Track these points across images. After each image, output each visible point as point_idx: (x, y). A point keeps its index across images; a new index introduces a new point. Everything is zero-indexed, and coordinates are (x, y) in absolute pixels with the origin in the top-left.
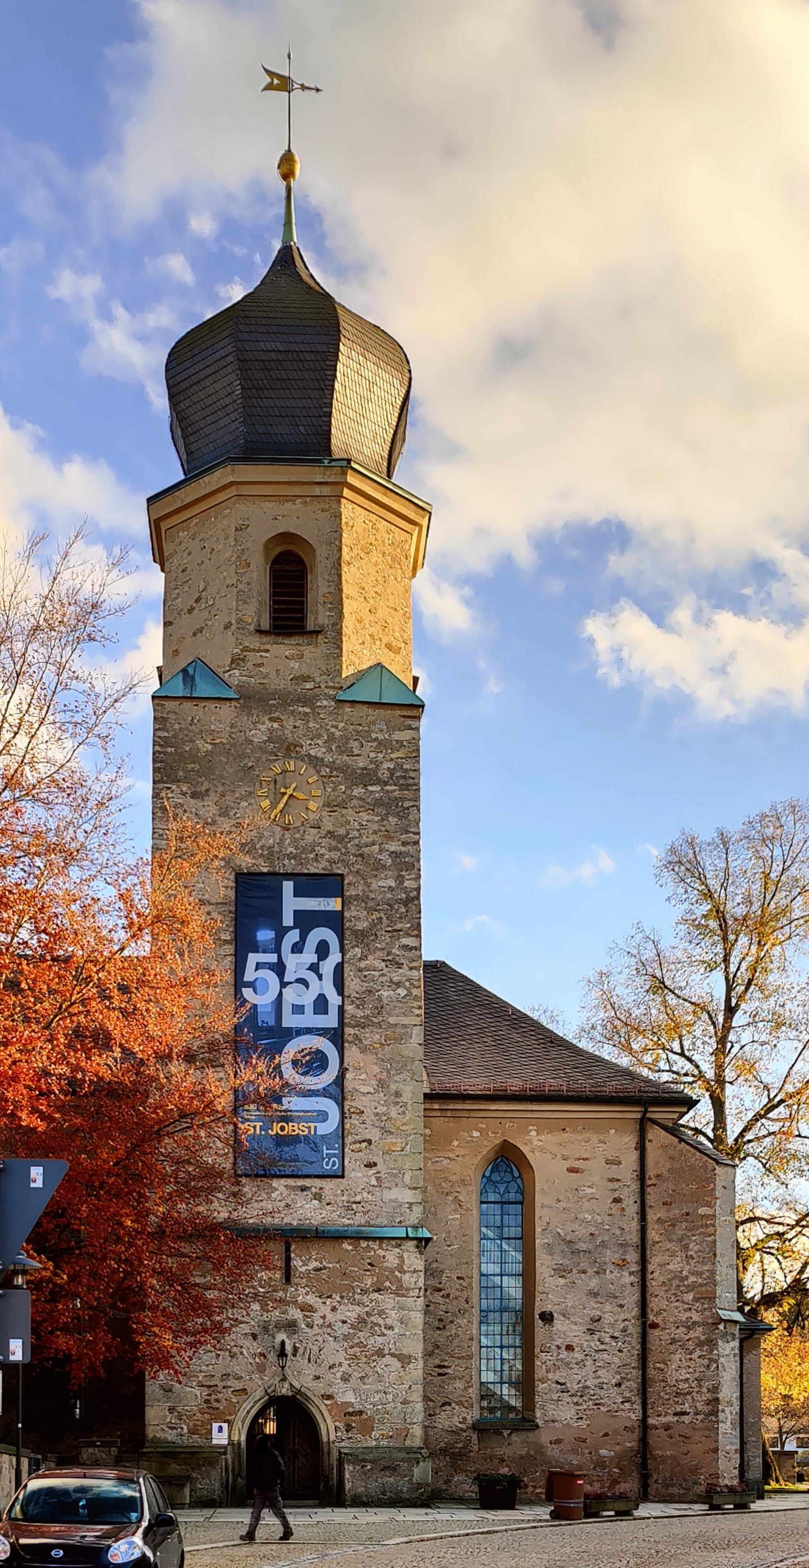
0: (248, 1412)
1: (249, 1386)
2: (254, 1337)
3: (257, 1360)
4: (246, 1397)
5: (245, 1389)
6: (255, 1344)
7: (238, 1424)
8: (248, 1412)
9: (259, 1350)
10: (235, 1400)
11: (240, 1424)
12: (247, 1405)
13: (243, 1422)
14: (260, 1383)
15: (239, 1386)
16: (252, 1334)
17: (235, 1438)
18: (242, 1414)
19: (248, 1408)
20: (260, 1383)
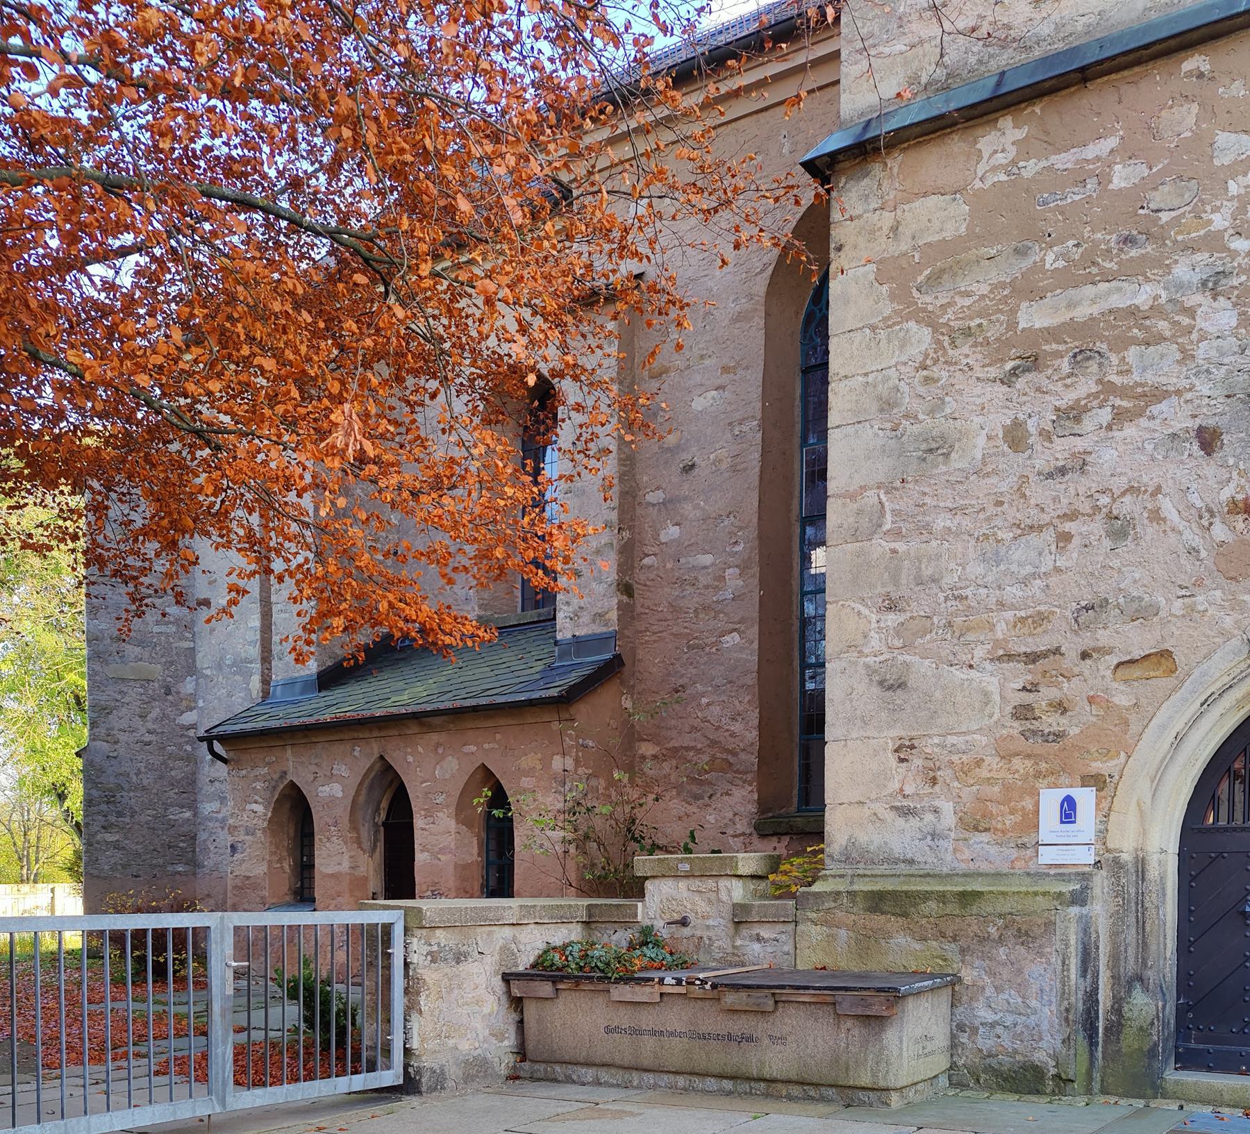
0: (1179, 739)
1: (1177, 637)
2: (1208, 440)
3: (1220, 532)
4: (1166, 683)
5: (1165, 654)
6: (1210, 469)
7: (1134, 787)
8: (1179, 739)
9: (1226, 493)
10: (1122, 699)
11: (1144, 786)
12: (1174, 712)
13: (1157, 781)
14: (1228, 622)
15: (1139, 641)
16: (1201, 431)
17: (1125, 844)
18: (1151, 747)
19: (1179, 725)
20: (1228, 622)
